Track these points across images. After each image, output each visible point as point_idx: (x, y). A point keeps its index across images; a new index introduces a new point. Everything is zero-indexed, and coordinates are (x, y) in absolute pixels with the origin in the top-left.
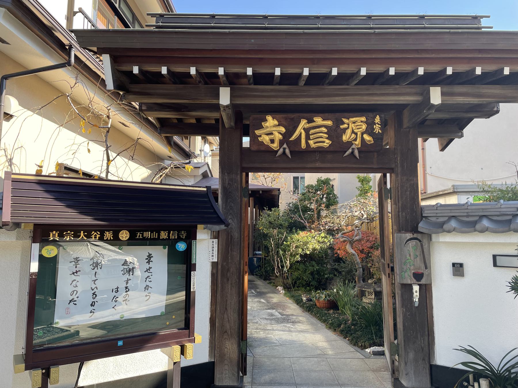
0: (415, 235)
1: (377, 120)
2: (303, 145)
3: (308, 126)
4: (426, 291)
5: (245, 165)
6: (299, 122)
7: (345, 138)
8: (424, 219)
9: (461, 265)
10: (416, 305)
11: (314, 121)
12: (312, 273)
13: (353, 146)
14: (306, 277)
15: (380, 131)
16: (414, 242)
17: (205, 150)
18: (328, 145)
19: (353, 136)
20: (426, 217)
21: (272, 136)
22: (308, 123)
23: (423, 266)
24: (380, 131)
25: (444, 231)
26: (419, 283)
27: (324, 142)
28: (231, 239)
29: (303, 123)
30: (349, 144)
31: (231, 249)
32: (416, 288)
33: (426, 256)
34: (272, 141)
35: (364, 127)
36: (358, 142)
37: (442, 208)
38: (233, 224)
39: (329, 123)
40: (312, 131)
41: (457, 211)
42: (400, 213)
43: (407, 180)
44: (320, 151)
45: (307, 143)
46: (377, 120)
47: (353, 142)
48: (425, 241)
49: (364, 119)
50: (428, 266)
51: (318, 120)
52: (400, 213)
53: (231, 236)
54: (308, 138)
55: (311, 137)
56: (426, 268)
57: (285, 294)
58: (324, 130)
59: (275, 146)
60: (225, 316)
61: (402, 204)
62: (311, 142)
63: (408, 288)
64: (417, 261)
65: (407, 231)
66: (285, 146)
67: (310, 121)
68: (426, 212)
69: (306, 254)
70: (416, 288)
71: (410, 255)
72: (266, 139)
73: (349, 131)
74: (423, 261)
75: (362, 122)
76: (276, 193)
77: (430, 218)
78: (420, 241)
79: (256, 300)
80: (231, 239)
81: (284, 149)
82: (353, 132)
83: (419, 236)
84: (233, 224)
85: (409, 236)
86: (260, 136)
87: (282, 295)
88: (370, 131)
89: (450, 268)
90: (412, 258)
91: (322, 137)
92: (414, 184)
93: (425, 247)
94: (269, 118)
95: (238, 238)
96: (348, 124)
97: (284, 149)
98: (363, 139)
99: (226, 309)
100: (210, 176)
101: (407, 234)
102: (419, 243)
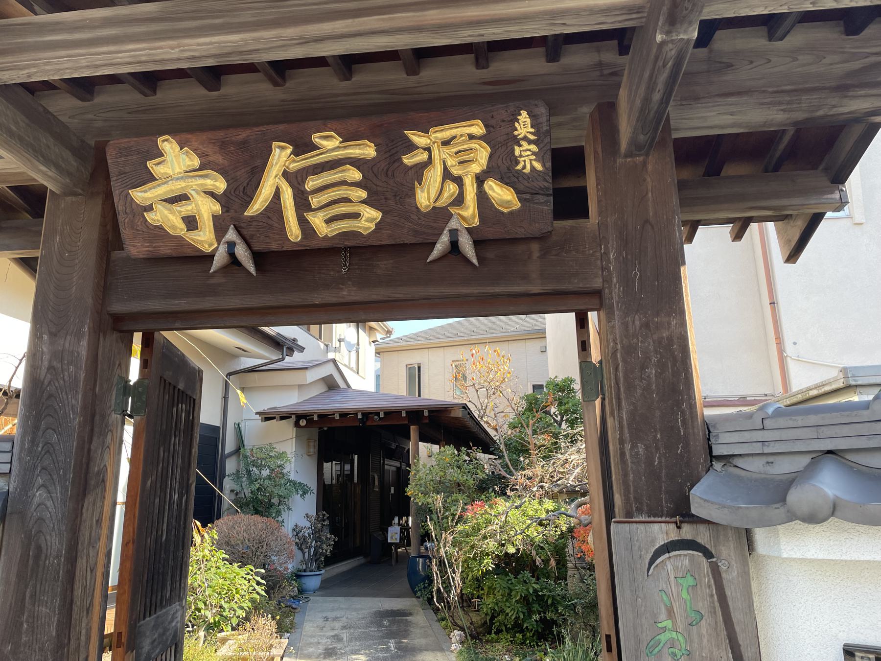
0: (687, 532)
1: (524, 126)
2: (294, 232)
3: (294, 166)
6: (269, 151)
7: (424, 198)
8: (718, 466)
11: (315, 147)
12: (525, 600)
13: (453, 224)
14: (512, 611)
15: (538, 166)
16: (684, 558)
17: (347, 339)
18: (372, 226)
19: (452, 188)
20: (726, 459)
21: (186, 209)
22: (297, 153)
24: (538, 166)
25: (792, 516)
27: (356, 216)
28: (37, 557)
29: (281, 157)
30: (441, 215)
31: (33, 596)
33: (737, 617)
34: (191, 222)
35: (482, 155)
36: (470, 210)
37: (782, 422)
38: (49, 503)
39: (368, 150)
40: (311, 184)
41: (846, 430)
42: (628, 446)
43: (646, 325)
44: (351, 251)
45: (303, 223)
46: (524, 126)
47: (452, 210)
48: (728, 553)
49: (478, 128)
51: (329, 144)
52: (628, 446)
53: (39, 548)
54: (302, 204)
55: (315, 201)
57: (461, 653)
58: (355, 175)
59: (204, 238)
61: (632, 414)
62: (317, 221)
64: (700, 635)
65: (655, 513)
66: (231, 235)
67: (303, 147)
68: (725, 438)
69: (507, 554)
71: (670, 613)
72: (168, 218)
73: (434, 176)
74: (723, 633)
75: (472, 137)
76: (458, 413)
77: (740, 462)
78: (708, 554)
80: (37, 557)
81: (231, 245)
82: (447, 175)
84: (49, 503)
85: (662, 532)
86: (150, 208)
88: (502, 168)
90: (681, 626)
91: (346, 200)
92: (670, 339)
93: (730, 576)
94: (168, 146)
95: (58, 556)
96: (428, 149)
97: (231, 245)
98: (482, 198)
100: (342, 385)
101: (656, 527)
102: (704, 562)
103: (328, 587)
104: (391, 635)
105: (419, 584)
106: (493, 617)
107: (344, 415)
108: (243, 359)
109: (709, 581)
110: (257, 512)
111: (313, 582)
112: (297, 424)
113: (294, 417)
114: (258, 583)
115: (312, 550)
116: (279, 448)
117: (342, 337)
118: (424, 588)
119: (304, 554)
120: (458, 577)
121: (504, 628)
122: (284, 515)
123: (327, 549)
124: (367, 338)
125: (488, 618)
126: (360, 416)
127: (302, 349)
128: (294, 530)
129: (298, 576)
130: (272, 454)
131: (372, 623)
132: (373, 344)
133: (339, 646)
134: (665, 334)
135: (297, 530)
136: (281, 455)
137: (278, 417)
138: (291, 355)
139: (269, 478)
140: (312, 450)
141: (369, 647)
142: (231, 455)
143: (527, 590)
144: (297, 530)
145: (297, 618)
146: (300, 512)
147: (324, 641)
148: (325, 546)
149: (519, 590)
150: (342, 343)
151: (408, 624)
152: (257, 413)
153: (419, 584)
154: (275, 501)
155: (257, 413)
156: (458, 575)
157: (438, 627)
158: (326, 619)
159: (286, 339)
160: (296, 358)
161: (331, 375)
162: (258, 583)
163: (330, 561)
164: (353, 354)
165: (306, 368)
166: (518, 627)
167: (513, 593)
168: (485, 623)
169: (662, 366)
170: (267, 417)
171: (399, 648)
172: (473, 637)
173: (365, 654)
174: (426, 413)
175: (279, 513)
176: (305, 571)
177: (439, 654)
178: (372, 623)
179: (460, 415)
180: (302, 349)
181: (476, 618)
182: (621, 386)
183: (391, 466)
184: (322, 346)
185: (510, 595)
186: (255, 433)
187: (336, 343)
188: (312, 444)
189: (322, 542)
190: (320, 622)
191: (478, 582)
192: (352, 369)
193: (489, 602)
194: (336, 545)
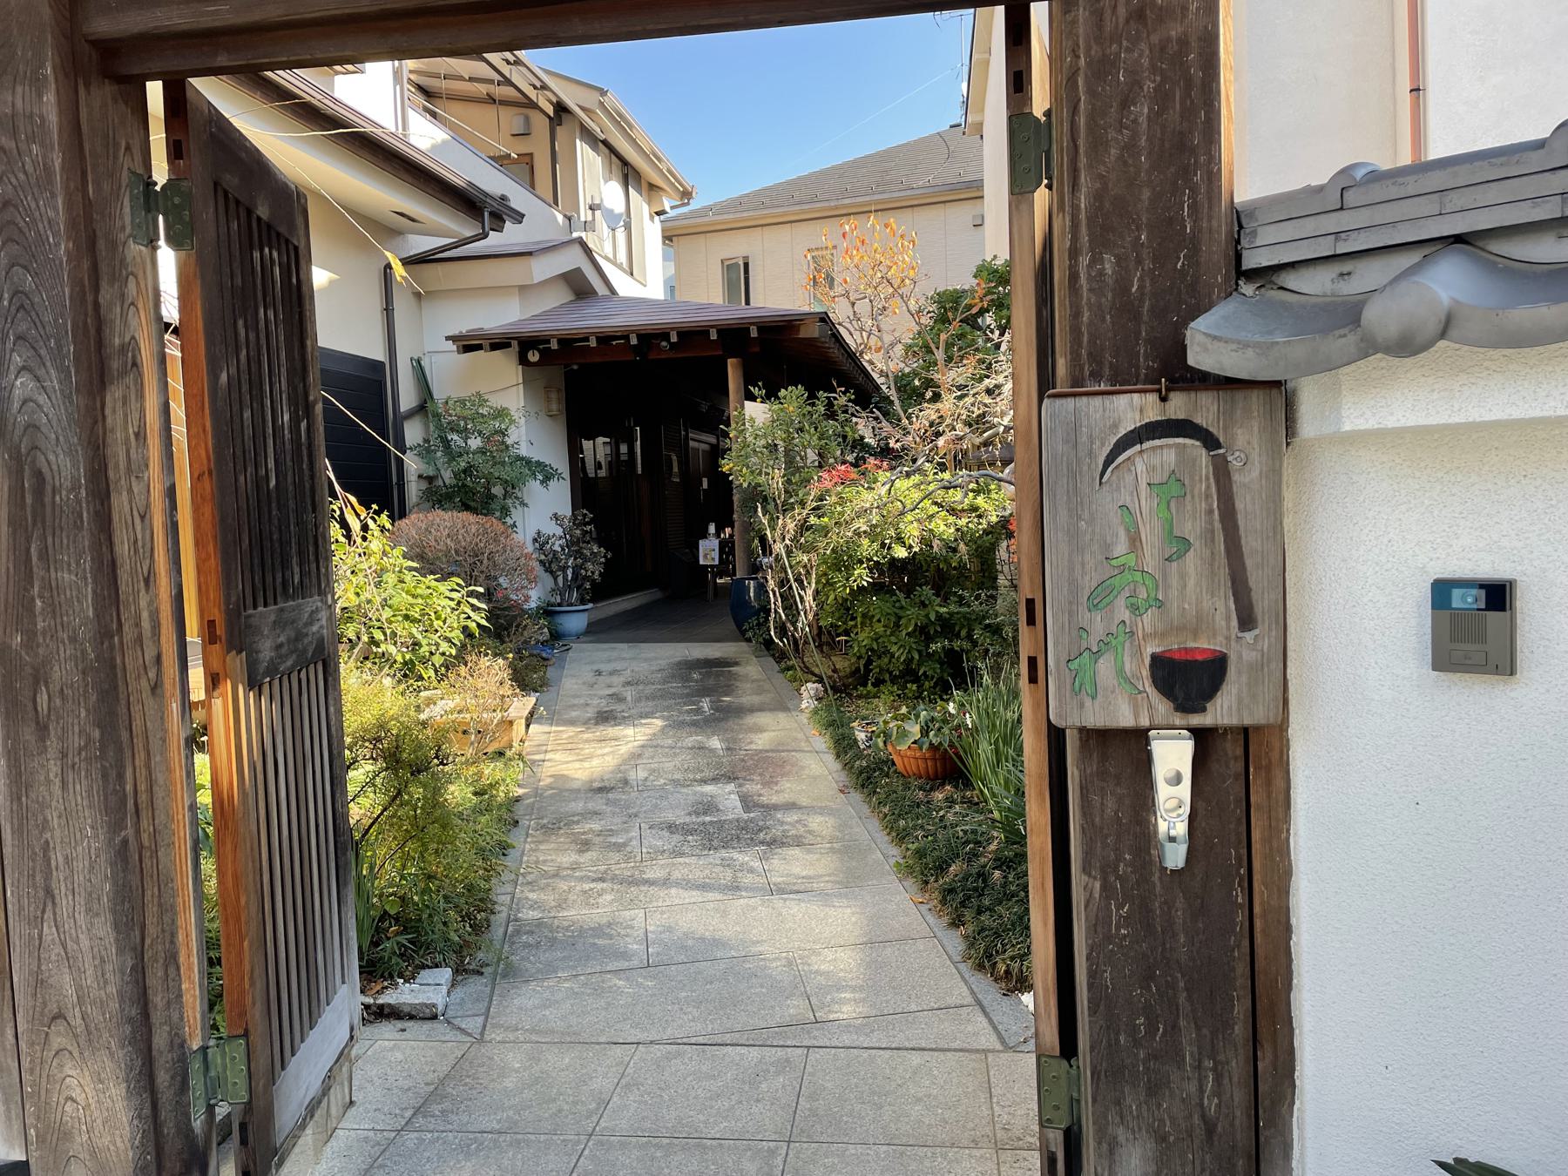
0: (1179, 406)
4: (1244, 771)
5: (104, 26)
8: (1248, 289)
9: (1498, 595)
10: (1175, 857)
12: (924, 633)
16: (1166, 452)
17: (608, 204)
20: (1265, 275)
23: (1223, 608)
25: (1370, 347)
26: (1196, 720)
28: (39, 491)
31: (44, 555)
32: (1172, 756)
33: (1251, 543)
38: (42, 399)
41: (1493, 194)
42: (1084, 260)
48: (1246, 439)
50: (1262, 603)
52: (1084, 260)
53: (39, 476)
56: (1247, 620)
57: (815, 712)
60: (49, 931)
61: (1098, 197)
63: (1127, 750)
64: (1183, 576)
65: (1123, 380)
68: (1266, 235)
69: (893, 561)
70: (1172, 756)
71: (1135, 541)
74: (1223, 573)
76: (812, 331)
77: (1291, 280)
78: (1210, 442)
79: (691, 741)
80: (39, 491)
83: (1204, 409)
84: (42, 399)
85: (1134, 408)
87: (804, 718)
89: (1413, 622)
90: (1151, 563)
92: (1183, 42)
93: (1247, 479)
95: (75, 488)
99: (49, 893)
100: (601, 289)
101: (1122, 400)
102: (1202, 456)
103: (598, 631)
104: (704, 692)
105: (746, 617)
106: (869, 662)
107: (605, 339)
108: (412, 238)
109: (1208, 487)
110: (466, 507)
111: (575, 622)
112: (523, 360)
113: (515, 343)
114: (475, 608)
115: (570, 572)
116: (496, 401)
117: (597, 201)
118: (759, 625)
119: (555, 579)
120: (809, 598)
121: (887, 677)
122: (516, 515)
123: (594, 570)
124: (645, 207)
125: (862, 662)
126: (634, 341)
127: (519, 217)
128: (535, 540)
129: (548, 612)
130: (484, 411)
131: (673, 676)
132: (657, 218)
133: (619, 707)
134: (1175, 31)
135: (540, 541)
136: (501, 413)
137: (486, 343)
138: (500, 229)
139: (482, 451)
140: (554, 406)
141: (668, 708)
142: (411, 414)
143: (927, 616)
144: (540, 541)
145: (551, 673)
146: (544, 511)
147: (596, 702)
148: (589, 566)
149: (913, 617)
150: (598, 213)
151: (731, 675)
152: (448, 338)
153: (746, 617)
154: (497, 490)
155: (448, 338)
156: (810, 592)
157: (780, 680)
158: (599, 673)
159: (486, 195)
160: (509, 237)
161: (578, 270)
162: (475, 608)
163: (599, 592)
164: (621, 234)
165: (530, 254)
166: (909, 674)
167: (903, 621)
168: (858, 669)
169: (1162, 98)
170: (468, 344)
171: (717, 708)
172: (835, 689)
173: (662, 717)
174: (754, 333)
175: (505, 512)
176: (559, 605)
177: (781, 716)
178: (673, 676)
179: (816, 335)
180: (519, 217)
181: (842, 664)
182: (1081, 142)
183: (700, 442)
184: (560, 218)
185: (897, 625)
186: (453, 377)
187: (585, 214)
188: (554, 396)
189: (586, 560)
190: (589, 677)
191: (845, 607)
192: (620, 266)
193: (864, 637)
194: (607, 564)
